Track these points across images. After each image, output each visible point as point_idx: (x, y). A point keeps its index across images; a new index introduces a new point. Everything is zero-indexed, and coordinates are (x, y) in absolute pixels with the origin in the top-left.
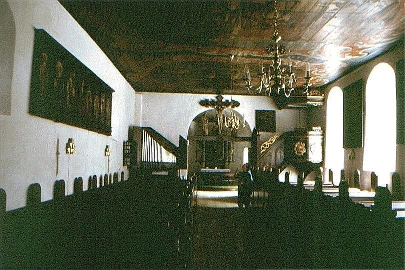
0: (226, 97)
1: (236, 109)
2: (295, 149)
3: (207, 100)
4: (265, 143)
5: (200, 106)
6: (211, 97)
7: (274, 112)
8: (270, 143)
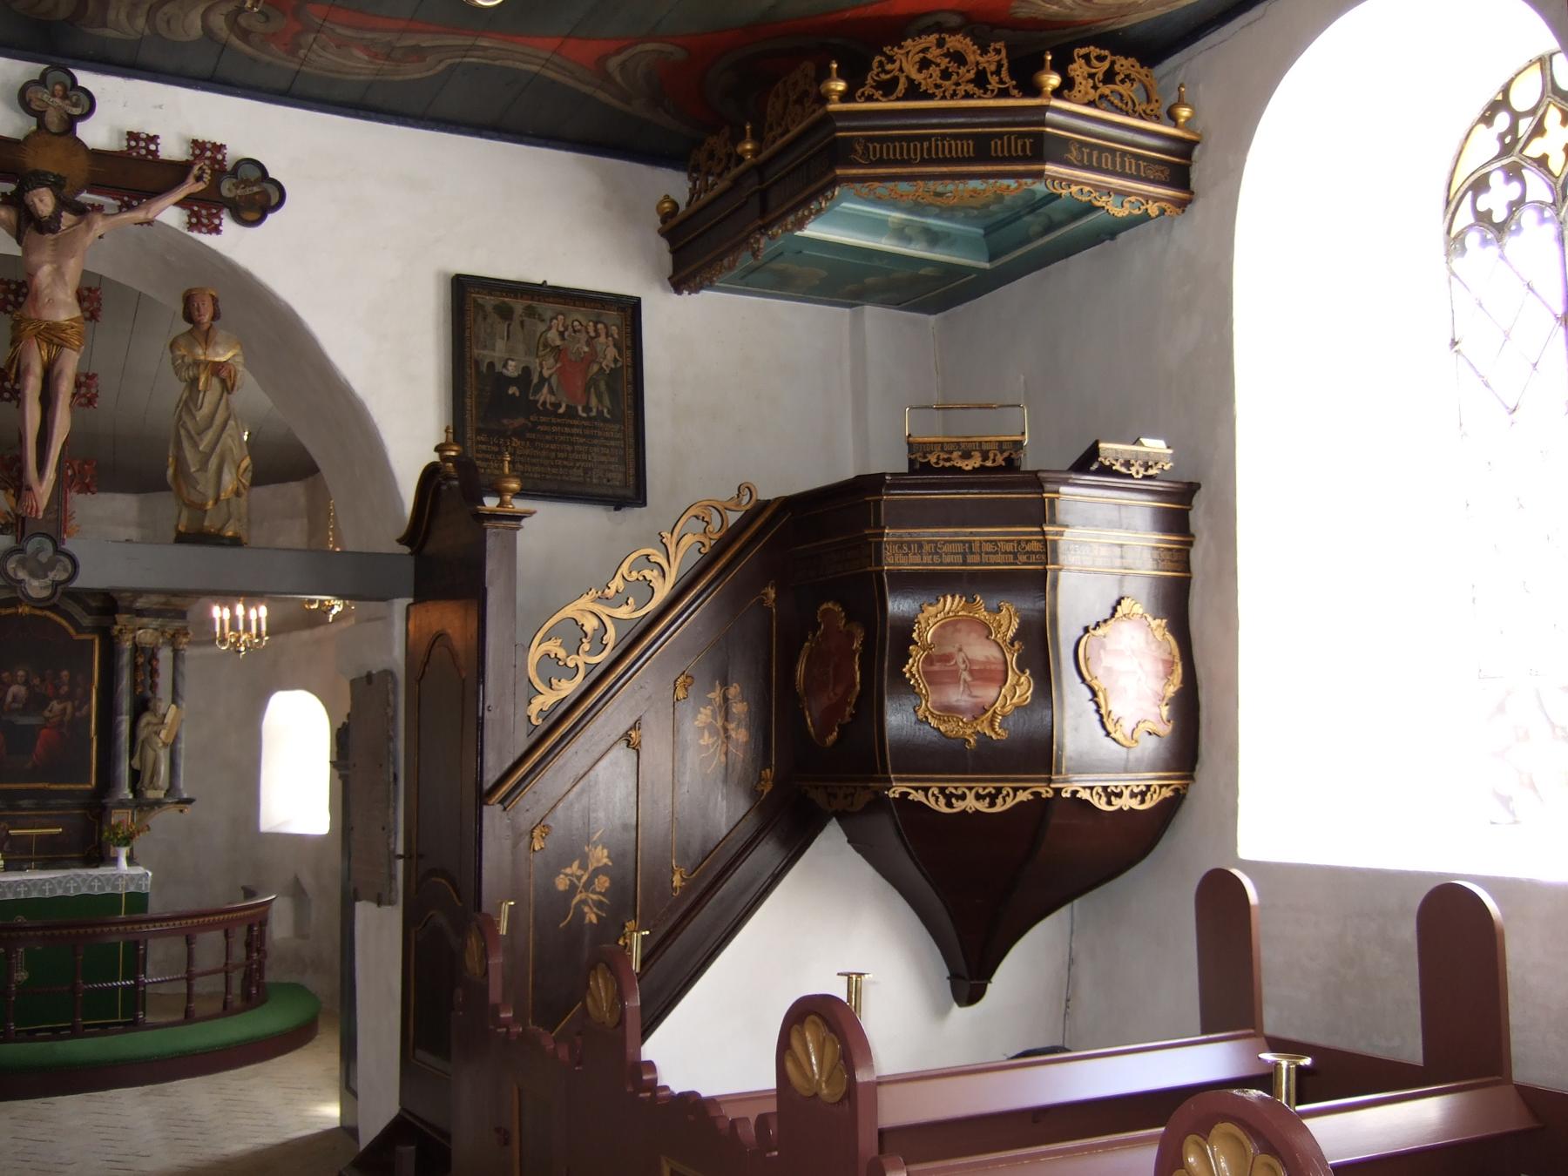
0: (121, 109)
2: (914, 666)
4: (568, 611)
7: (630, 309)
8: (623, 612)
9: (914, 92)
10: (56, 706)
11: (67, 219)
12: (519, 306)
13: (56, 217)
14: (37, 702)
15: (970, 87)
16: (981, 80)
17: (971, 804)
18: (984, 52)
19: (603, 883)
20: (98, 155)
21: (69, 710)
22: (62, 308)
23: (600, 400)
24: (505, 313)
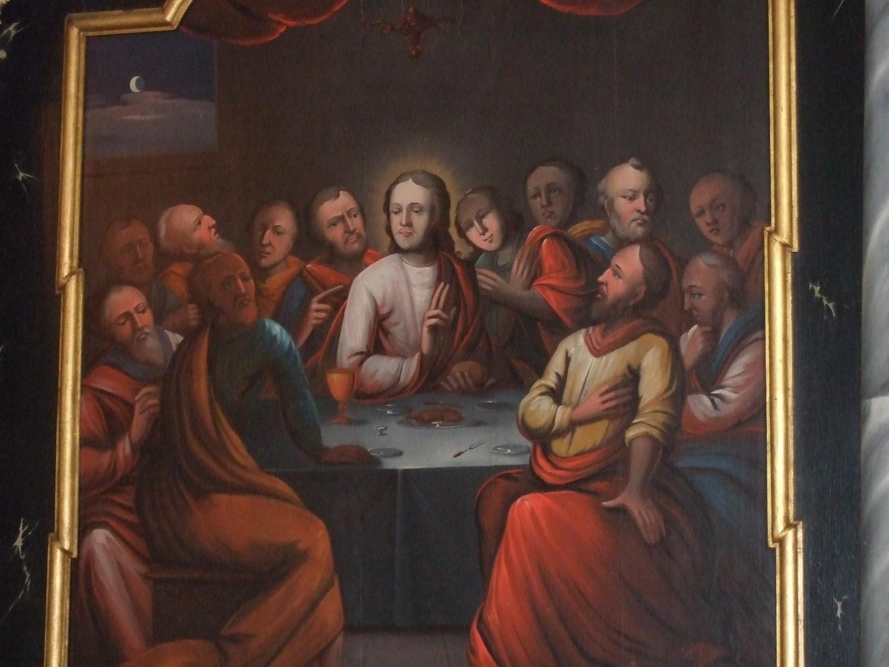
10: (584, 363)
14: (488, 347)
21: (653, 384)
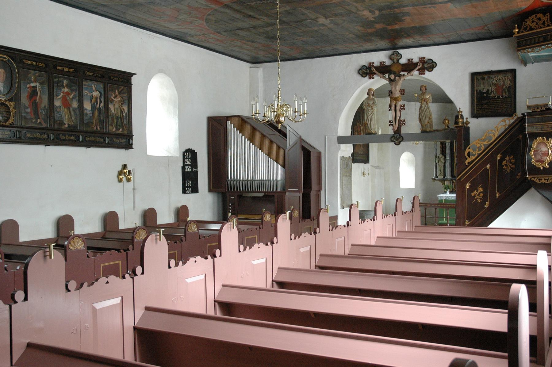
0: (408, 55)
1: (428, 75)
3: (371, 65)
5: (359, 77)
6: (380, 57)
7: (513, 72)
8: (485, 143)
9: (531, 29)
11: (397, 78)
12: (486, 77)
13: (395, 79)
15: (541, 25)
16: (544, 23)
17: (543, 181)
18: (545, 16)
19: (481, 195)
20: (403, 65)
22: (397, 94)
23: (505, 93)
24: (483, 79)
